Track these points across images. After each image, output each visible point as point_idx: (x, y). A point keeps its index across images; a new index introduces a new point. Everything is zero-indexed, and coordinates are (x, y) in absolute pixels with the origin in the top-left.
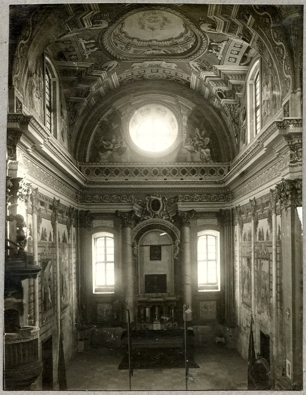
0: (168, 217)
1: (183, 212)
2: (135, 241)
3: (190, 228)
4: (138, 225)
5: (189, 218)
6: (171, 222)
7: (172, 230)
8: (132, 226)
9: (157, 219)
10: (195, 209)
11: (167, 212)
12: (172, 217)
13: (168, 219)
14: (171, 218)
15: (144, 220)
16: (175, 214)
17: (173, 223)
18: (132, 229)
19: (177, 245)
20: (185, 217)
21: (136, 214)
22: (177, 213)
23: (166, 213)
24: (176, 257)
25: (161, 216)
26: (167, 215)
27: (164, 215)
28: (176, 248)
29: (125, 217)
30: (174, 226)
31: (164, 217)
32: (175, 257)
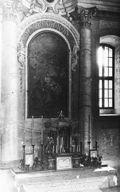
0: (65, 13)
1: (83, 9)
2: (21, 43)
3: (91, 30)
4: (26, 19)
5: (91, 17)
6: (69, 20)
7: (70, 31)
8: (18, 19)
9: (50, 14)
10: (97, 6)
11: (64, 6)
12: (70, 14)
13: (65, 16)
14: (69, 15)
15: (33, 13)
16: (73, 10)
17: (71, 22)
18: (17, 24)
19: (76, 52)
20: (86, 15)
21: (23, 4)
22: (76, 9)
23: (63, 8)
24: (74, 68)
25: (56, 11)
26: (64, 10)
27: (61, 9)
28: (75, 57)
29: (9, 5)
30: (72, 26)
31: (60, 13)
32: (72, 69)
